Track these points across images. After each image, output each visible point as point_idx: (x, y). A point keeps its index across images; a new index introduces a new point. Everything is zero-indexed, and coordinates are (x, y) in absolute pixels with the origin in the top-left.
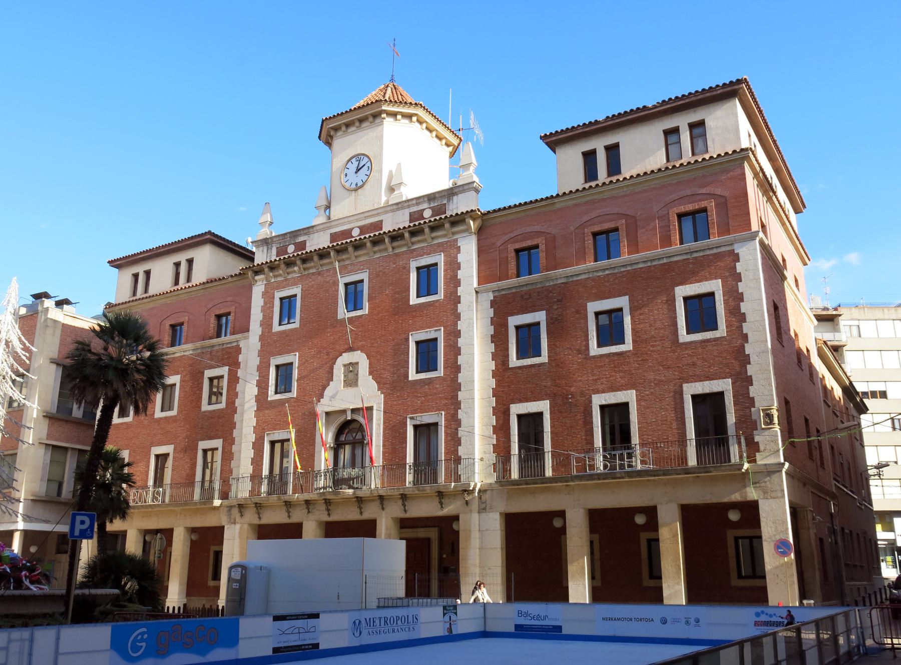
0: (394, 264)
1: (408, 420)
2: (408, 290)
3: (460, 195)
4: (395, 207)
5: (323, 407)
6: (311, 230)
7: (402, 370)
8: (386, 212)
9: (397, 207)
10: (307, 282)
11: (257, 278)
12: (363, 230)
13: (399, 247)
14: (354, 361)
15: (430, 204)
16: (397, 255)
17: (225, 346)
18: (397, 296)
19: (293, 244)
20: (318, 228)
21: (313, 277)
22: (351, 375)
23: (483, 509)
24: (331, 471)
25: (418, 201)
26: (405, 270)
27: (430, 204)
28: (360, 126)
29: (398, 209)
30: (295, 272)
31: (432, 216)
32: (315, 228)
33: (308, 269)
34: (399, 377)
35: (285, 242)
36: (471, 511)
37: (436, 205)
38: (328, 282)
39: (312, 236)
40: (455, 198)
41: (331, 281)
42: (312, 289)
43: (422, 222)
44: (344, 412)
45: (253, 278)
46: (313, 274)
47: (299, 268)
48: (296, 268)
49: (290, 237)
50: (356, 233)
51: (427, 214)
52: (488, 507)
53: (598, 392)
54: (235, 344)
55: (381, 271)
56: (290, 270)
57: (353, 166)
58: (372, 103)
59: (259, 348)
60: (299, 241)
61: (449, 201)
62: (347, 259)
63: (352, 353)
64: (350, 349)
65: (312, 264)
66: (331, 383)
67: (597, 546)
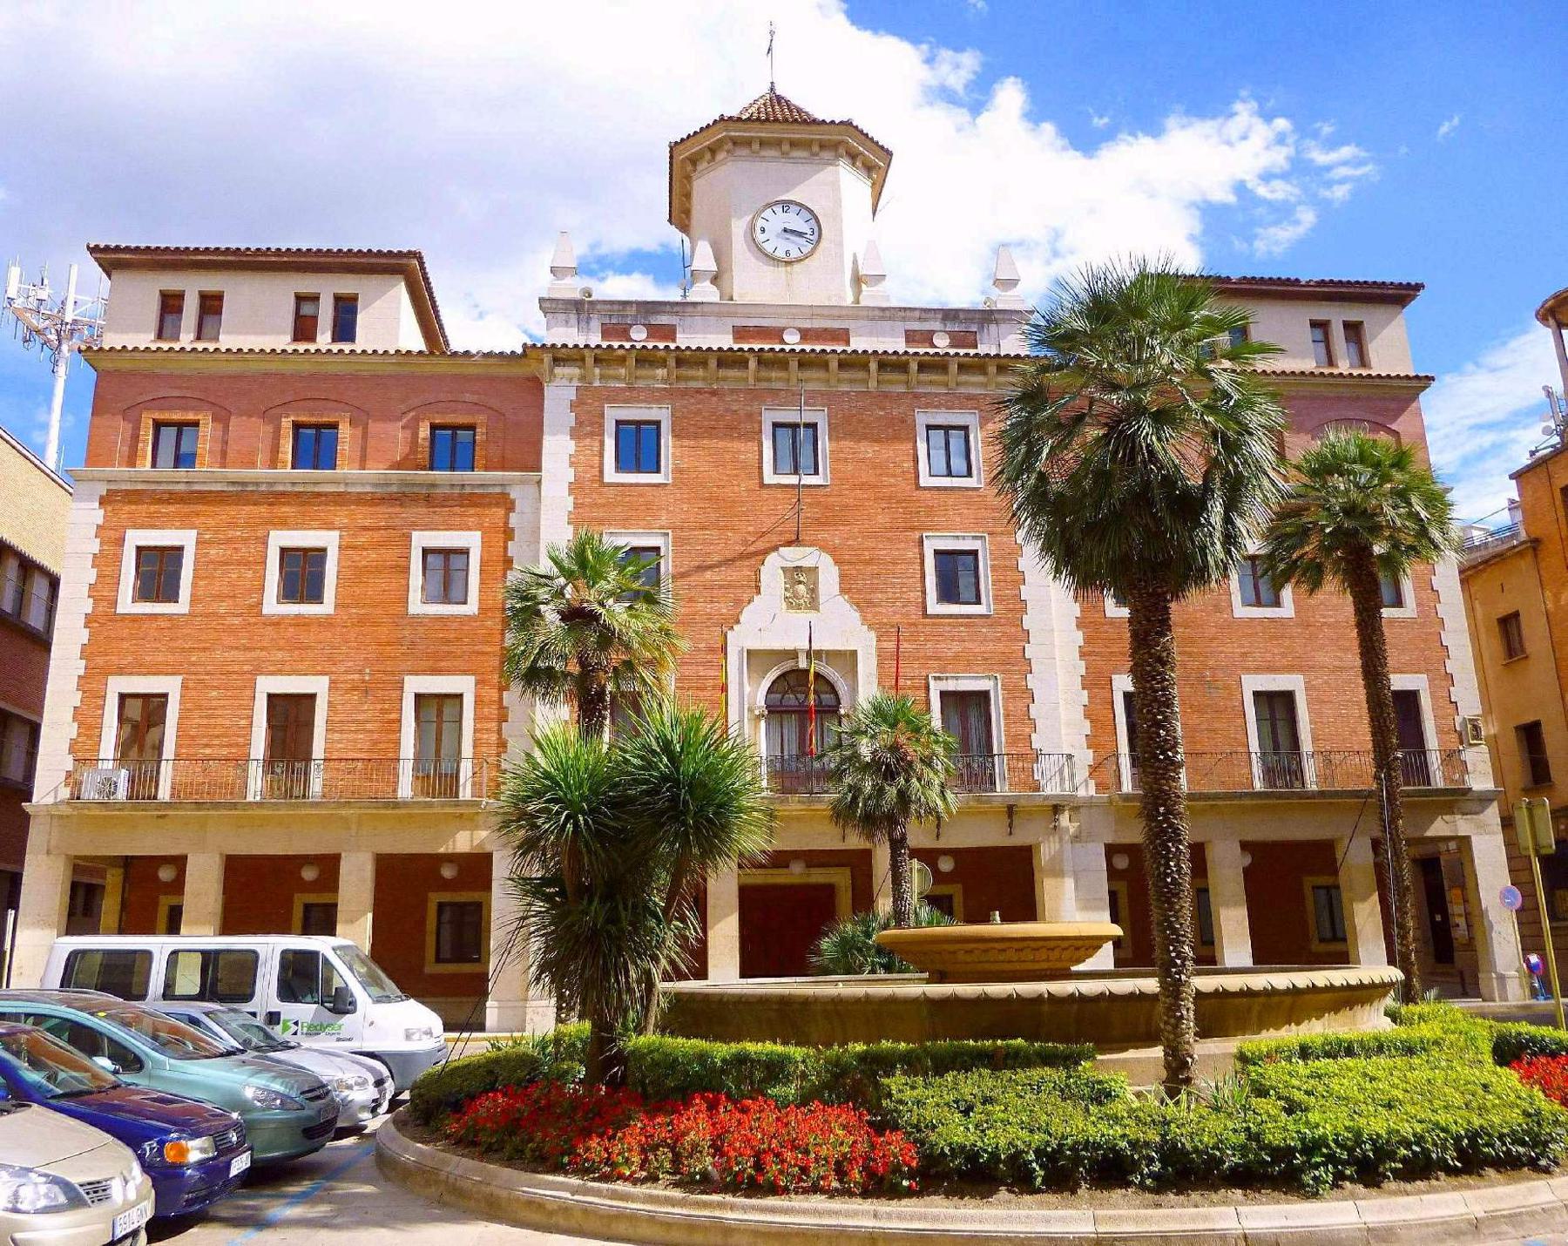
4: (877, 313)
5: (743, 638)
6: (690, 309)
8: (856, 318)
11: (558, 370)
13: (890, 382)
14: (806, 563)
16: (886, 395)
17: (468, 490)
28: (817, 155)
29: (882, 318)
30: (654, 378)
32: (699, 308)
40: (993, 327)
41: (742, 413)
44: (793, 654)
45: (551, 371)
46: (699, 391)
48: (661, 372)
53: (1248, 670)
54: (498, 490)
56: (640, 372)
57: (797, 222)
58: (758, 119)
59: (571, 508)
62: (779, 379)
65: (701, 373)
67: (1123, 901)
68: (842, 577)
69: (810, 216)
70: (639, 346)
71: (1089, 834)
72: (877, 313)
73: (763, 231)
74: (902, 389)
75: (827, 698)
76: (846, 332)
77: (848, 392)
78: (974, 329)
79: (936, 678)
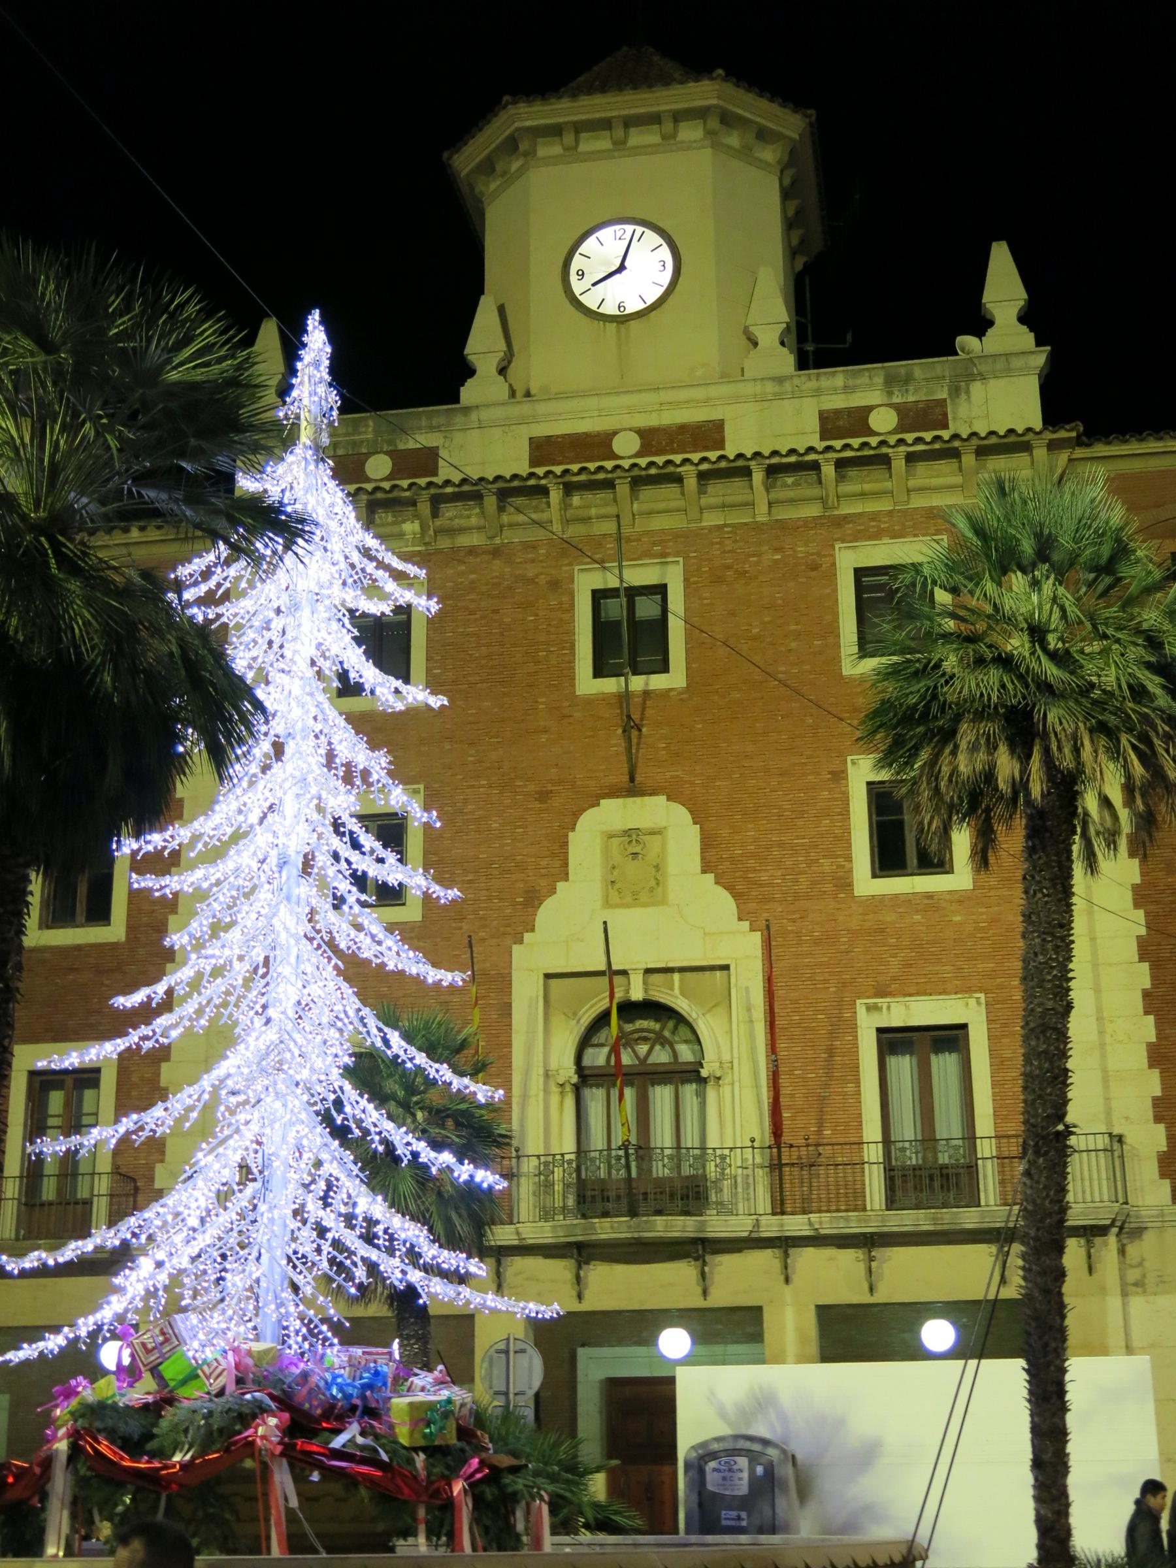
0: (777, 550)
1: (861, 1011)
2: (833, 631)
3: (992, 383)
7: (826, 865)
9: (777, 389)
10: (450, 572)
12: (650, 439)
14: (645, 823)
15: (890, 394)
18: (793, 645)
19: (386, 453)
20: (485, 415)
21: (471, 559)
22: (632, 869)
23: (1136, 1284)
24: (570, 1162)
25: (851, 382)
26: (814, 574)
27: (890, 394)
31: (639, 455)
33: (452, 532)
34: (814, 883)
35: (355, 444)
36: (1103, 1290)
37: (911, 399)
38: (532, 581)
39: (458, 437)
40: (977, 388)
41: (542, 580)
42: (473, 596)
43: (609, 465)
46: (472, 551)
47: (424, 528)
49: (375, 431)
50: (626, 445)
51: (883, 421)
52: (1151, 1279)
55: (728, 567)
60: (411, 445)
61: (955, 391)
63: (638, 800)
64: (633, 788)
66: (560, 885)
68: (707, 843)
69: (660, 241)
70: (626, 464)
71: (1161, 1281)
72: (770, 387)
73: (581, 274)
74: (812, 511)
75: (686, 1053)
76: (719, 426)
77: (719, 528)
78: (942, 394)
79: (869, 1008)
